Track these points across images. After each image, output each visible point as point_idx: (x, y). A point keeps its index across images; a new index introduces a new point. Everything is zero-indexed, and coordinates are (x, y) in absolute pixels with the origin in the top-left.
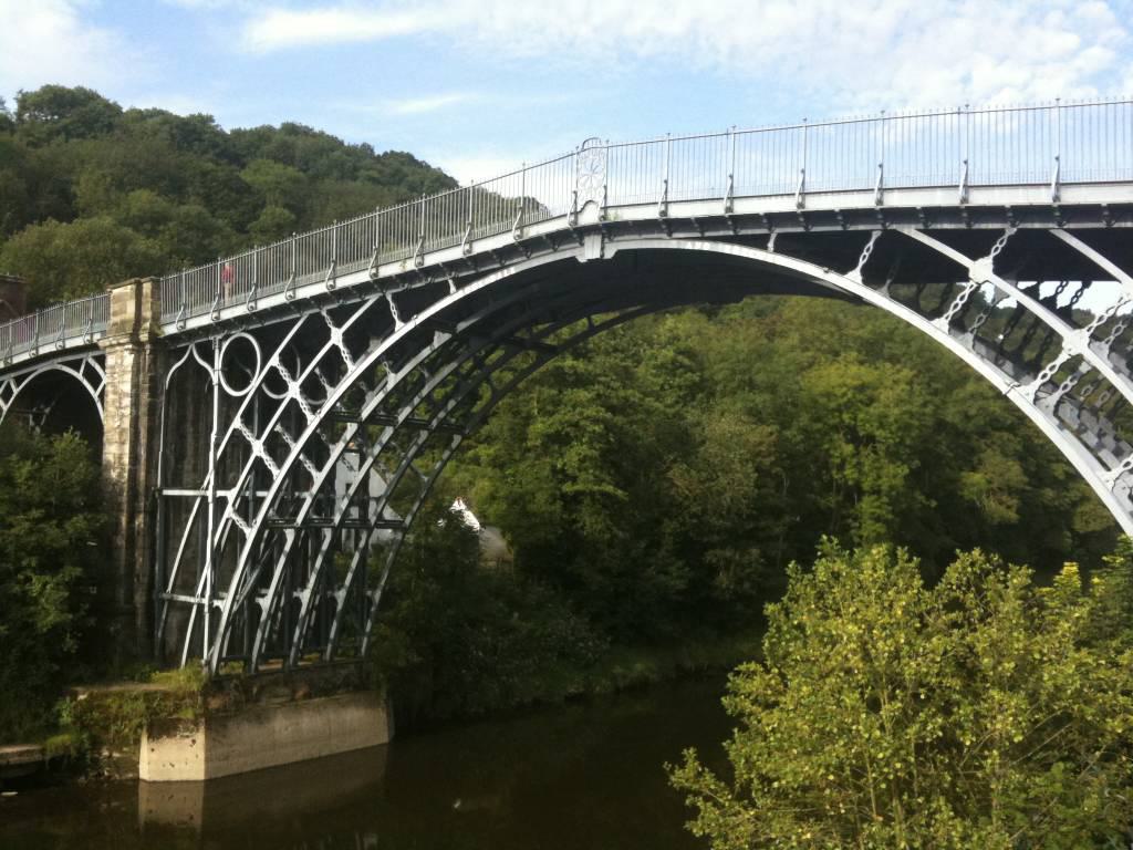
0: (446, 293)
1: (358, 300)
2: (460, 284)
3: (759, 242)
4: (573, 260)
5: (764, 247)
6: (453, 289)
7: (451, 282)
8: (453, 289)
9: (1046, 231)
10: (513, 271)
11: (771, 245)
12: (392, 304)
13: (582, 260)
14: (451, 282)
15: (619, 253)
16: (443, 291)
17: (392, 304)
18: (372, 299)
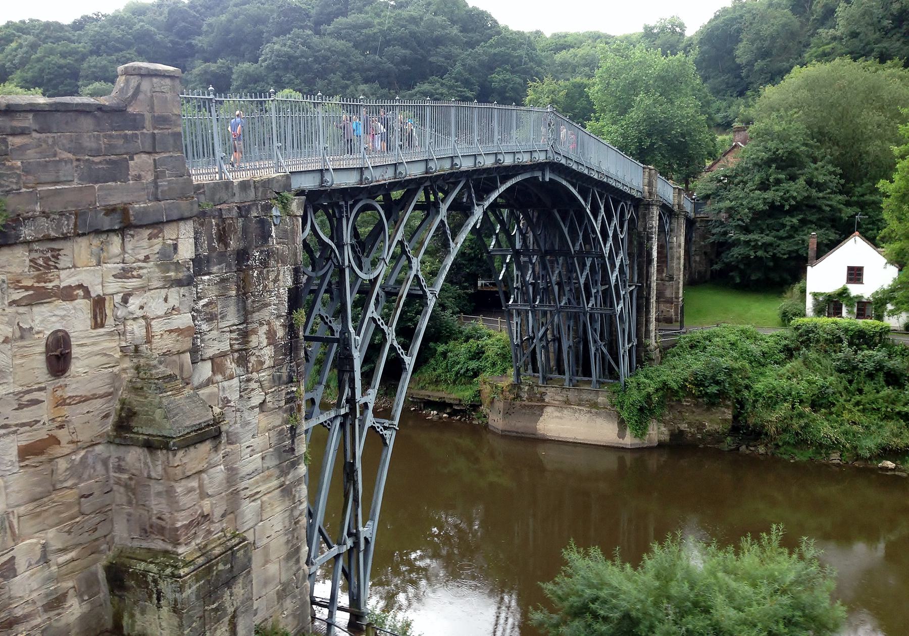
0: (497, 188)
2: (502, 183)
4: (537, 177)
5: (575, 188)
6: (499, 184)
8: (499, 184)
13: (541, 180)
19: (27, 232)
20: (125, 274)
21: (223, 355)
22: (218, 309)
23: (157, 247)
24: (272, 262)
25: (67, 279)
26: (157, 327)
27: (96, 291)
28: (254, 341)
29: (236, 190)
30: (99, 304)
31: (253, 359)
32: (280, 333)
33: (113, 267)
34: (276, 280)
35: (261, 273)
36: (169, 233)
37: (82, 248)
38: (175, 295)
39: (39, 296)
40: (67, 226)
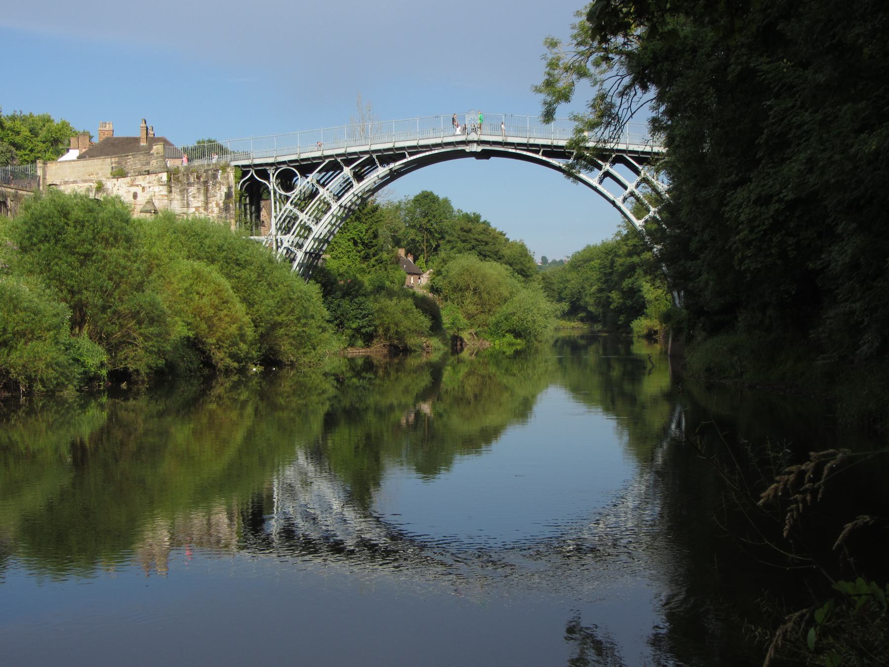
1: (357, 156)
2: (411, 154)
3: (537, 152)
6: (407, 156)
7: (406, 153)
8: (407, 156)
9: (622, 156)
10: (436, 152)
11: (541, 153)
12: (376, 160)
13: (468, 151)
14: (406, 153)
15: (483, 150)
16: (403, 156)
17: (376, 160)
18: (366, 157)
19: (129, 175)
20: (149, 183)
21: (199, 207)
22: (197, 195)
23: (157, 177)
24: (218, 185)
25: (137, 183)
26: (156, 194)
27: (143, 185)
28: (210, 205)
29: (206, 166)
30: (143, 188)
31: (210, 210)
32: (222, 205)
33: (148, 181)
34: (219, 190)
35: (213, 187)
36: (160, 175)
37: (140, 177)
38: (161, 188)
39: (132, 185)
40: (137, 174)
